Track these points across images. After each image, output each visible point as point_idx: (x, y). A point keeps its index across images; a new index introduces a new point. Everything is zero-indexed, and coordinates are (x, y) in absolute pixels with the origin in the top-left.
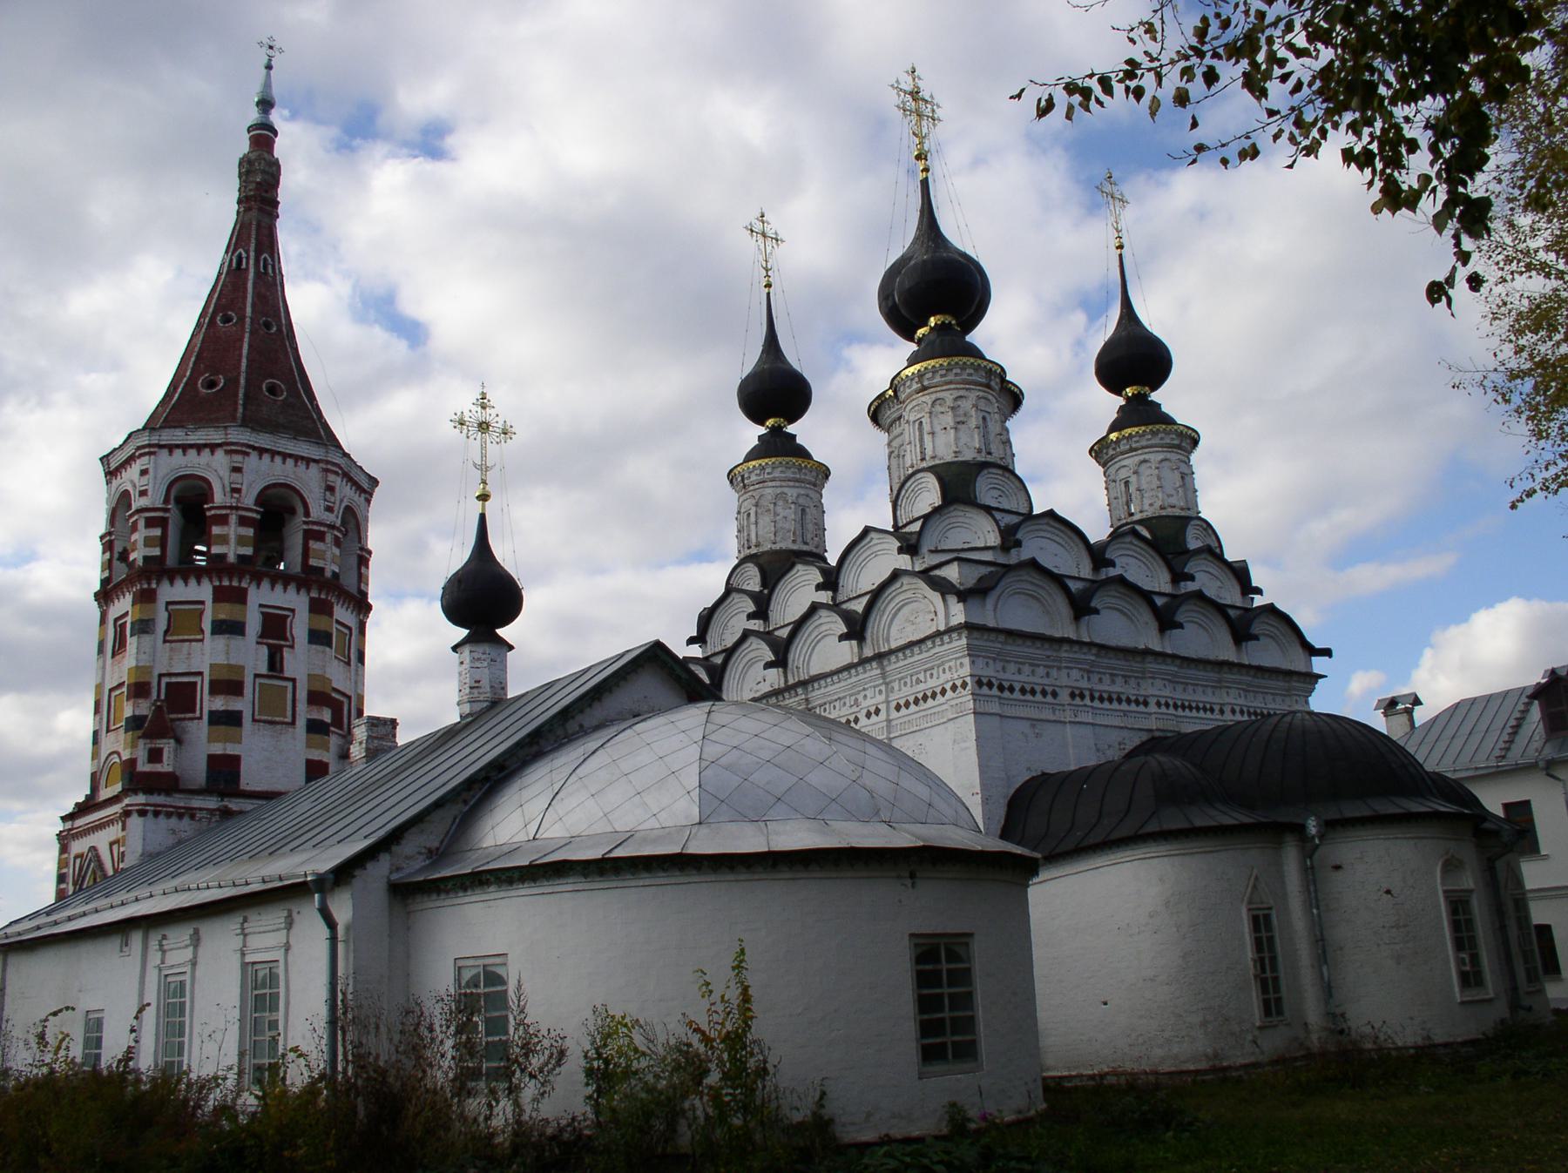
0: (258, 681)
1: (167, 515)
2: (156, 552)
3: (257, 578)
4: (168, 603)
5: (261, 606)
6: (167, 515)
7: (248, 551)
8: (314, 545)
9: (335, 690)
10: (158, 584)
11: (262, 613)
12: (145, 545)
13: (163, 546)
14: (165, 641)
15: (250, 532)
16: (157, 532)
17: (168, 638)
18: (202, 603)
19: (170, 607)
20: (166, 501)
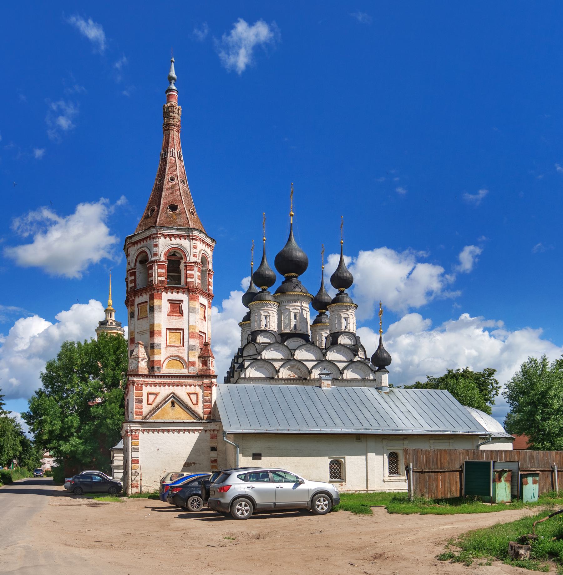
0: (168, 331)
1: (136, 270)
2: (133, 285)
3: (166, 290)
4: (138, 304)
5: (168, 300)
6: (136, 270)
7: (163, 279)
8: (188, 272)
9: (200, 332)
10: (135, 298)
11: (170, 303)
12: (130, 284)
13: (135, 281)
14: (138, 319)
15: (163, 271)
16: (133, 278)
17: (139, 318)
18: (146, 302)
19: (139, 306)
20: (135, 265)
